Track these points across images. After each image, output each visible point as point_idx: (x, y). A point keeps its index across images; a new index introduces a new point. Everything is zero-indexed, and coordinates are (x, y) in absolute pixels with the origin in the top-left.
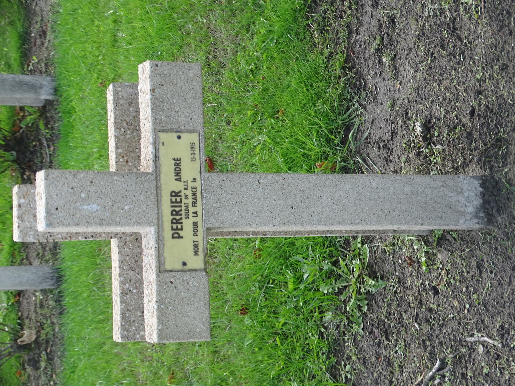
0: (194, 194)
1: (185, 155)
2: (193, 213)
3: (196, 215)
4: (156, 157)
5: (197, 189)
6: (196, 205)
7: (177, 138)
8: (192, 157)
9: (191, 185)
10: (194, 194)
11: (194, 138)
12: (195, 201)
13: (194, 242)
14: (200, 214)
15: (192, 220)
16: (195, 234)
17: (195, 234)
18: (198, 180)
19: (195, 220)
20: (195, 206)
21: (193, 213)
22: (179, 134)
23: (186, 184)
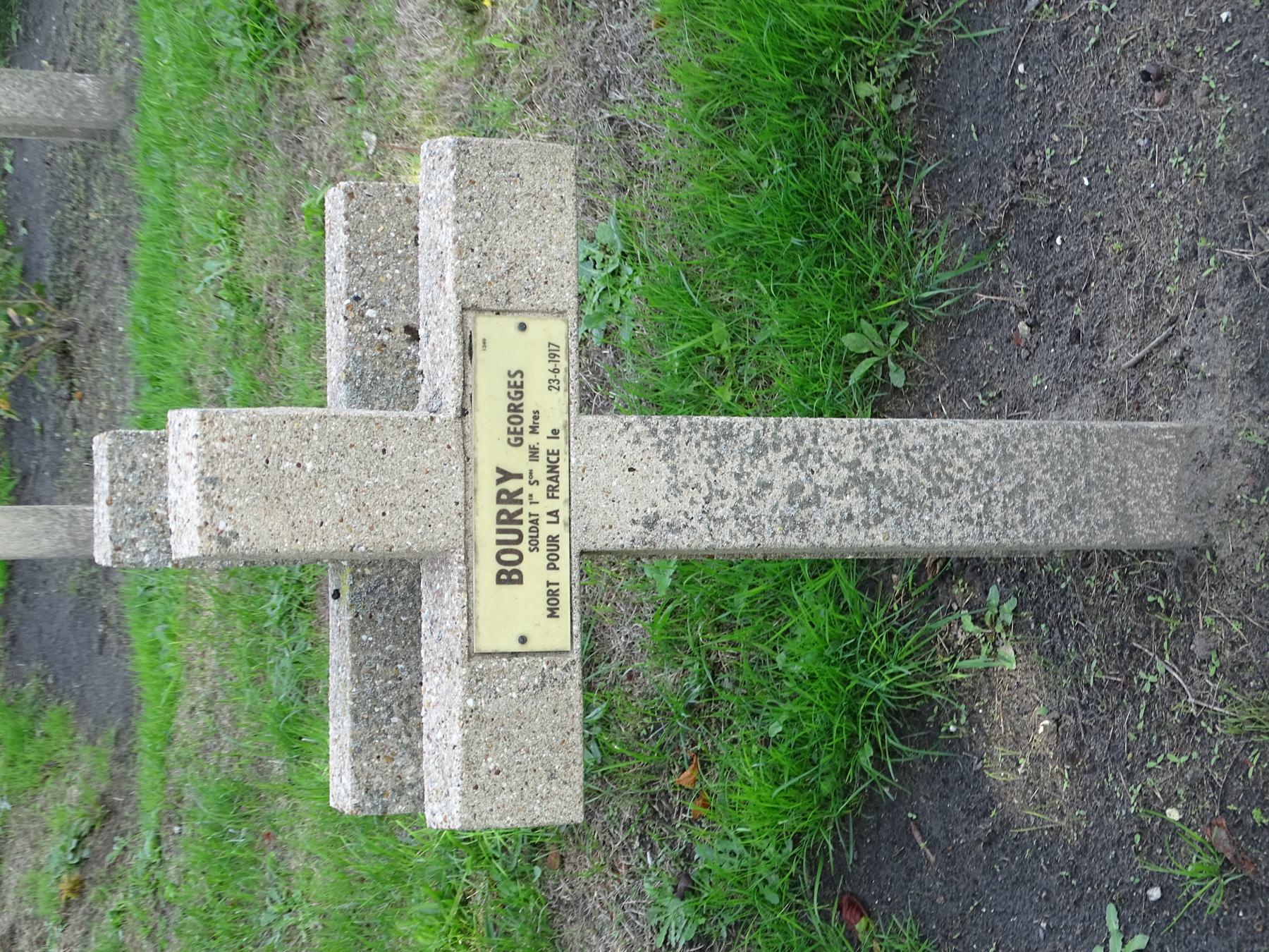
0: (553, 468)
2: (549, 514)
3: (555, 519)
5: (561, 456)
6: (556, 494)
8: (552, 376)
10: (553, 468)
12: (554, 484)
13: (548, 584)
14: (564, 515)
15: (545, 530)
16: (552, 566)
17: (552, 566)
20: (553, 497)
21: (549, 514)
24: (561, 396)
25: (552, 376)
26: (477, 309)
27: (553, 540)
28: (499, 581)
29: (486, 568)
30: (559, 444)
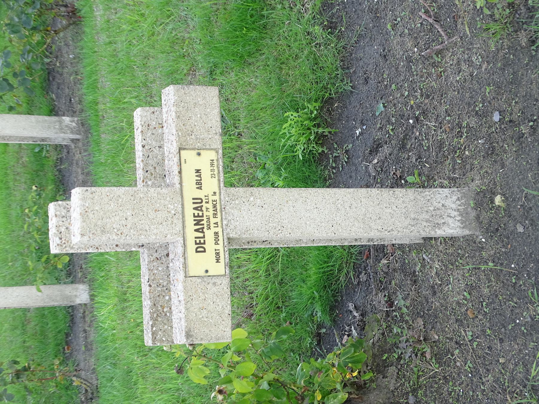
0: (215, 206)
2: (214, 224)
5: (218, 201)
7: (197, 157)
8: (212, 173)
9: (211, 198)
11: (212, 155)
13: (216, 250)
14: (219, 224)
15: (213, 230)
16: (216, 243)
17: (216, 243)
18: (217, 194)
19: (216, 230)
21: (214, 224)
22: (199, 151)
23: (207, 198)
24: (215, 180)
25: (212, 173)
28: (197, 252)
29: (191, 246)
30: (217, 198)
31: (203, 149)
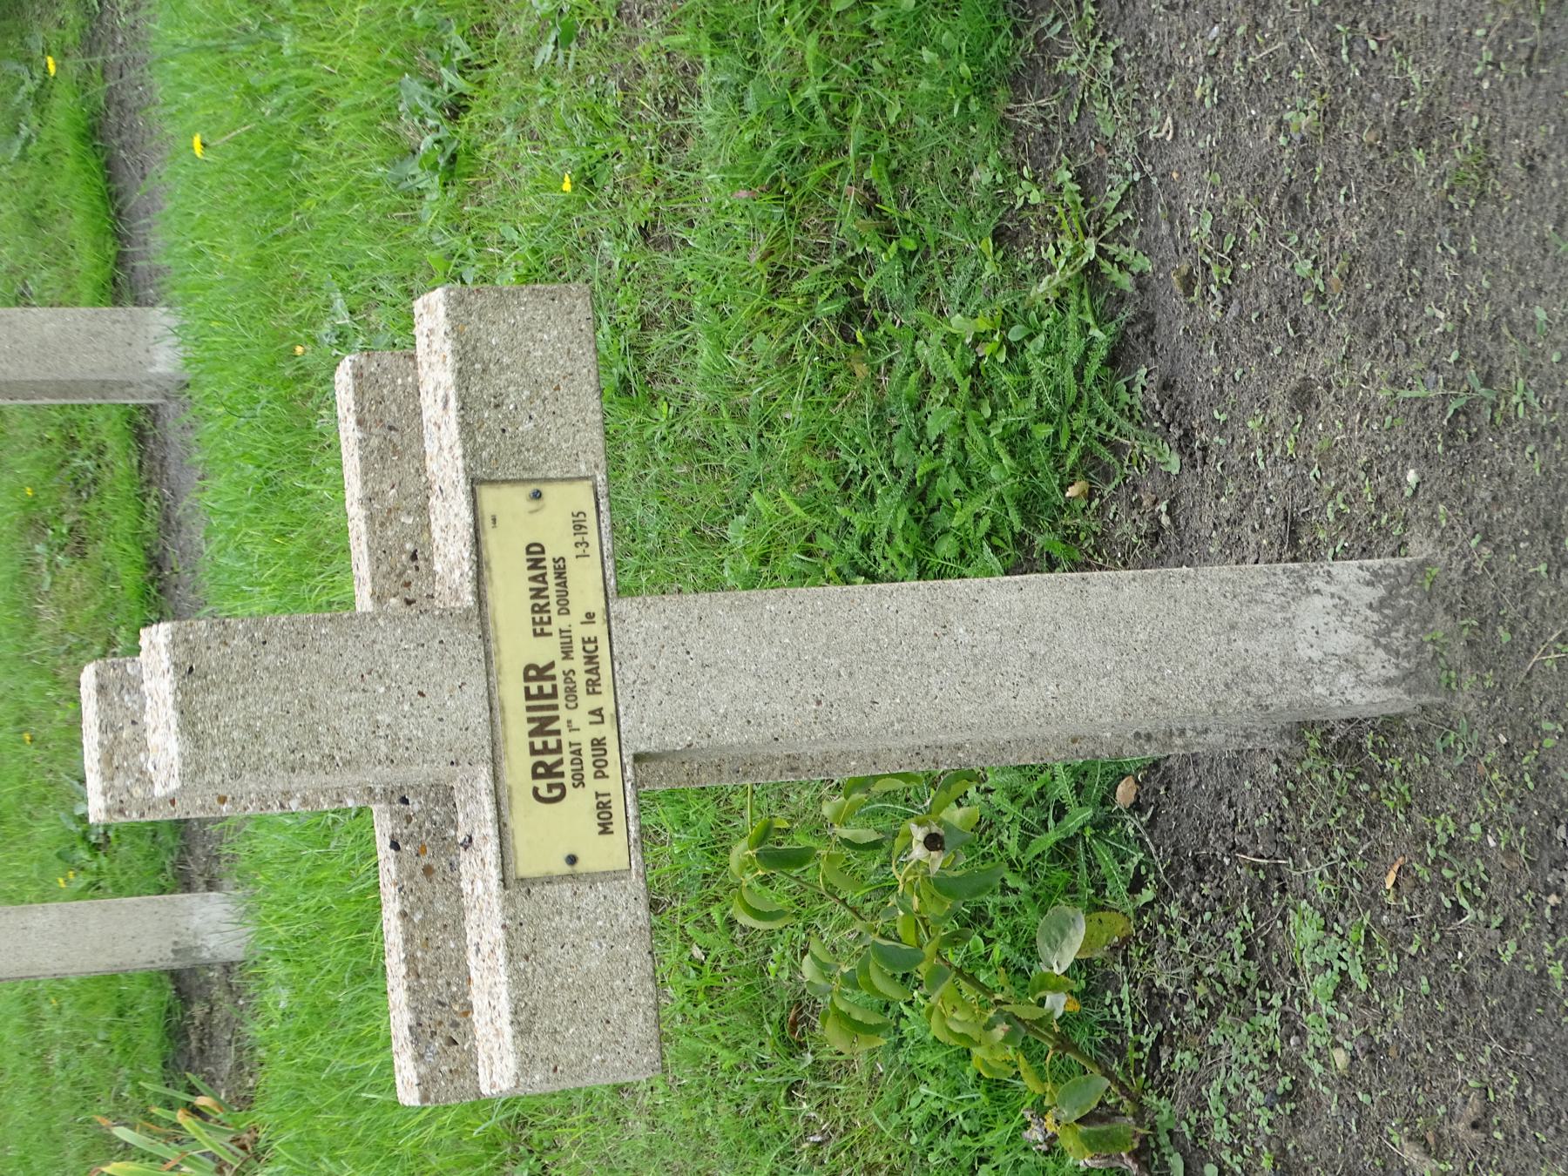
0: (591, 658)
1: (559, 544)
2: (592, 713)
4: (480, 565)
8: (580, 551)
10: (591, 658)
12: (594, 677)
14: (609, 710)
17: (600, 774)
18: (600, 618)
20: (594, 692)
21: (592, 713)
25: (580, 551)
26: (483, 482)
27: (598, 744)
31: (548, 480)
